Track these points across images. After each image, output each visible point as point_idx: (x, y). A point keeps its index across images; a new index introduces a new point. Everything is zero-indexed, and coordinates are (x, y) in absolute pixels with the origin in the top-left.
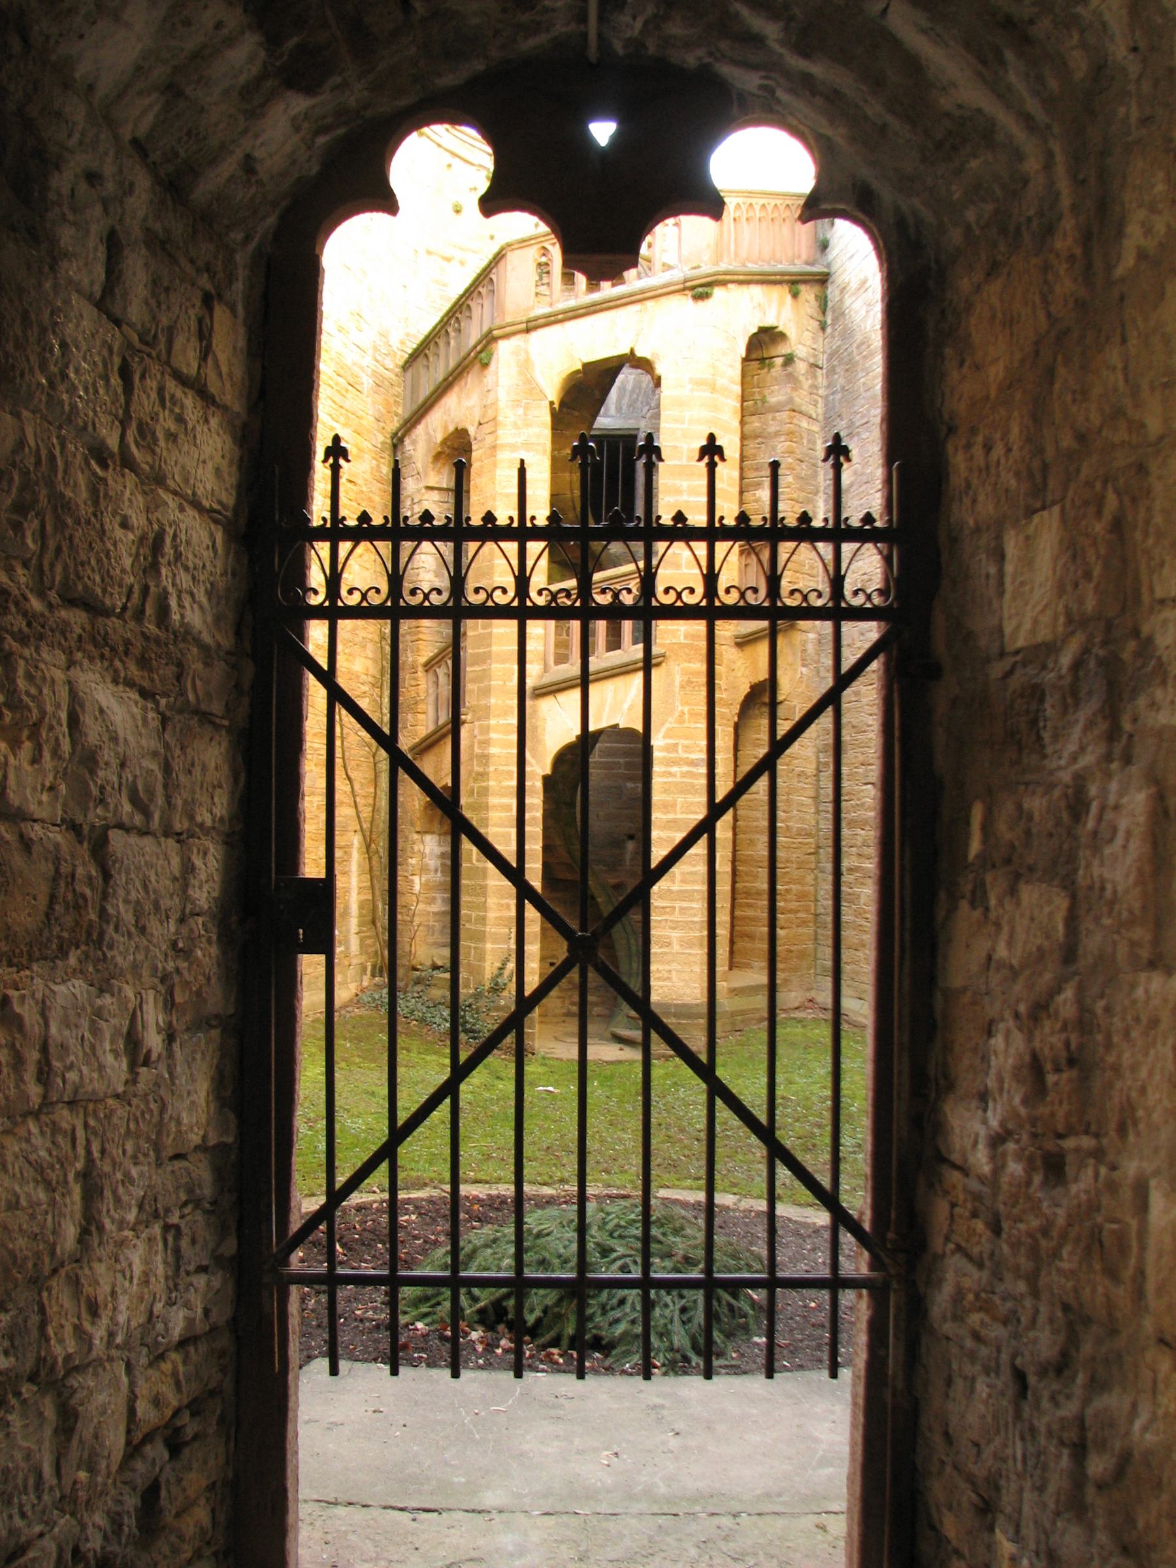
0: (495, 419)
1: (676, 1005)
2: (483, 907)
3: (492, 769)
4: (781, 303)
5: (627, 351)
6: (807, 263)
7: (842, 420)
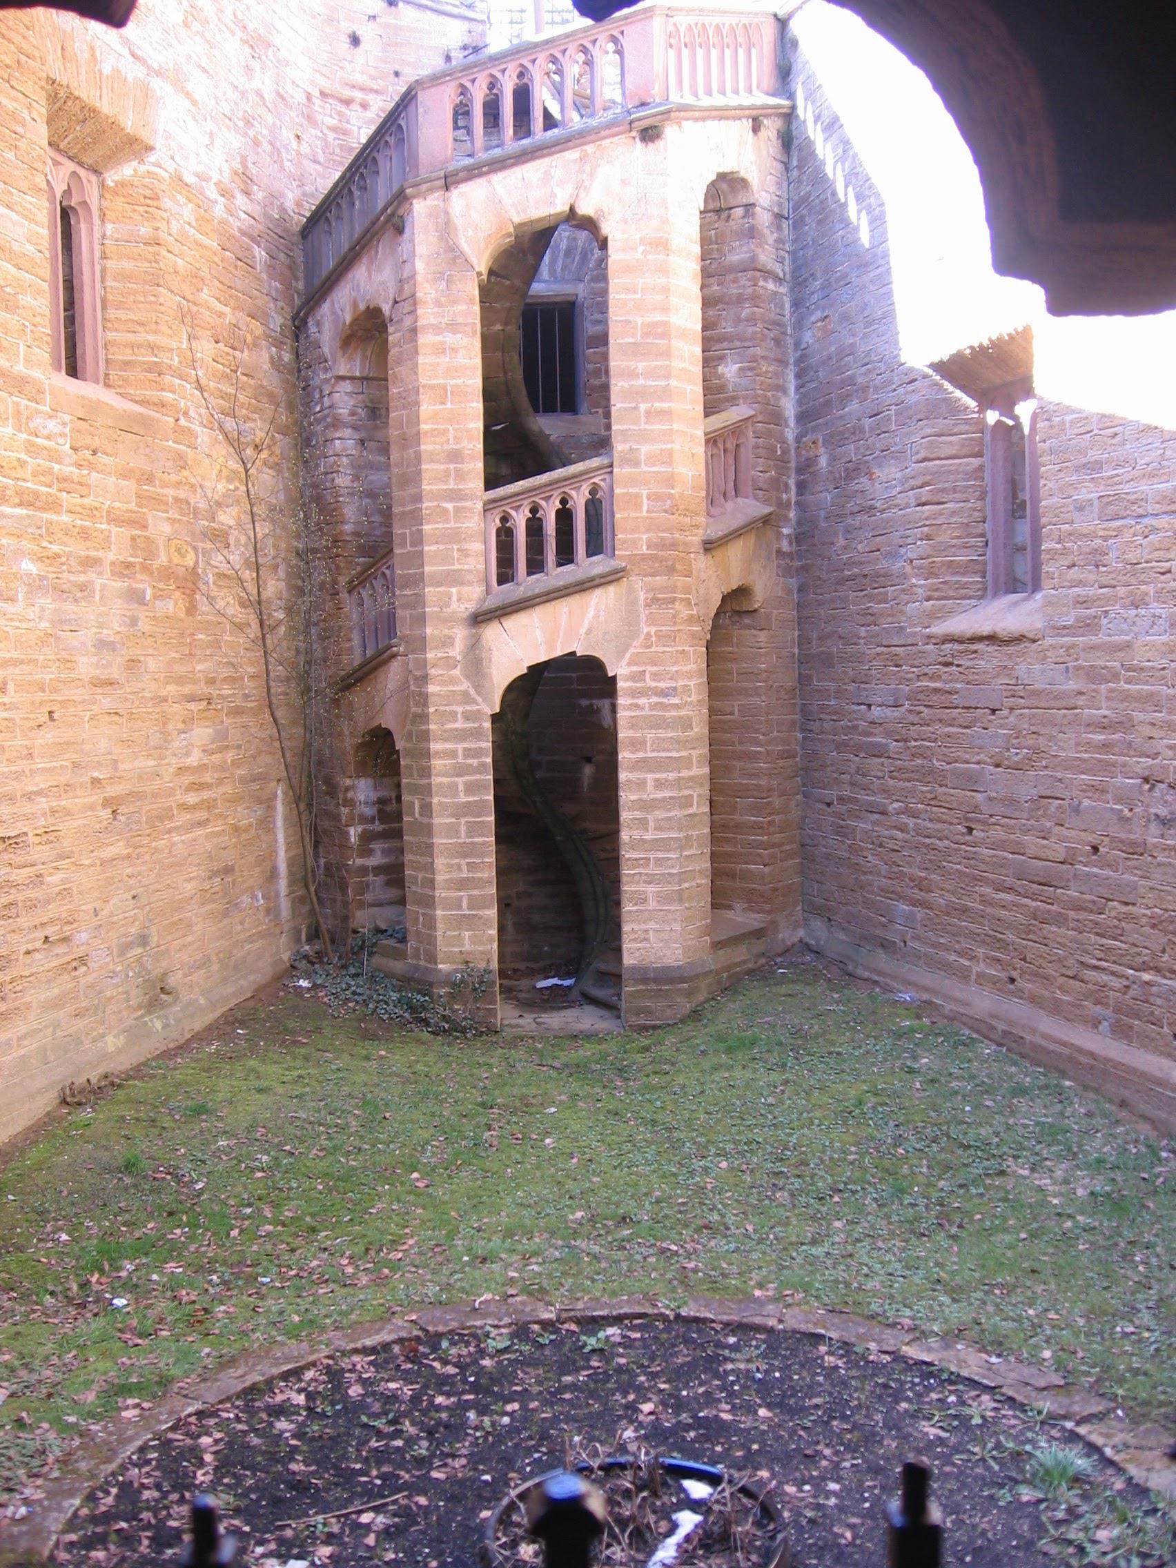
0: (413, 296)
1: (655, 969)
2: (431, 868)
3: (432, 710)
5: (567, 208)
7: (815, 279)
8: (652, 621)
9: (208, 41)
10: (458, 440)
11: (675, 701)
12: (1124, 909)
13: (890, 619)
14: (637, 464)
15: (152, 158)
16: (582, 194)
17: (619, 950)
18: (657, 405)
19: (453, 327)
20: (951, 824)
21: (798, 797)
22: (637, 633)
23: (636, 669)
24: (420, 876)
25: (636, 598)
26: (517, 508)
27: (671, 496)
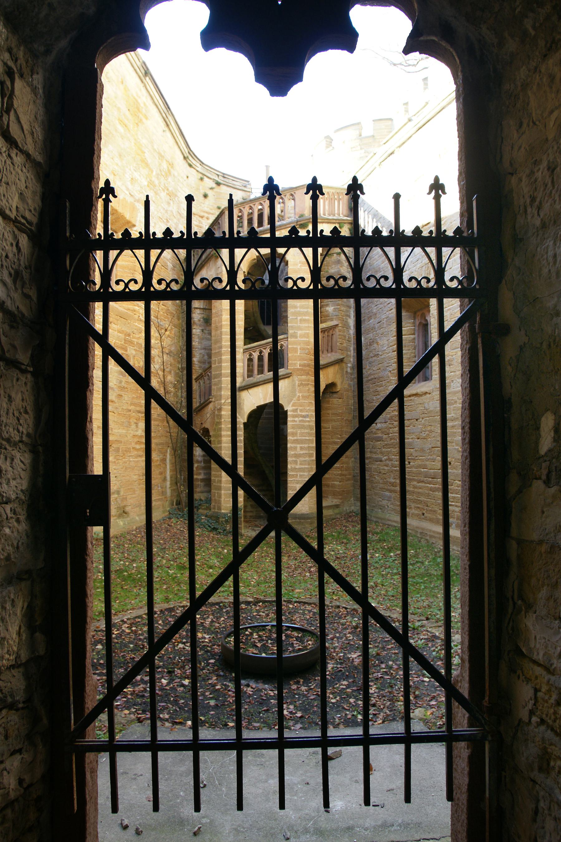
3: (223, 420)
8: (300, 392)
9: (155, 192)
11: (308, 419)
14: (296, 337)
18: (304, 317)
21: (353, 459)
22: (294, 396)
23: (294, 408)
24: (217, 479)
25: (295, 383)
26: (254, 352)
27: (308, 349)
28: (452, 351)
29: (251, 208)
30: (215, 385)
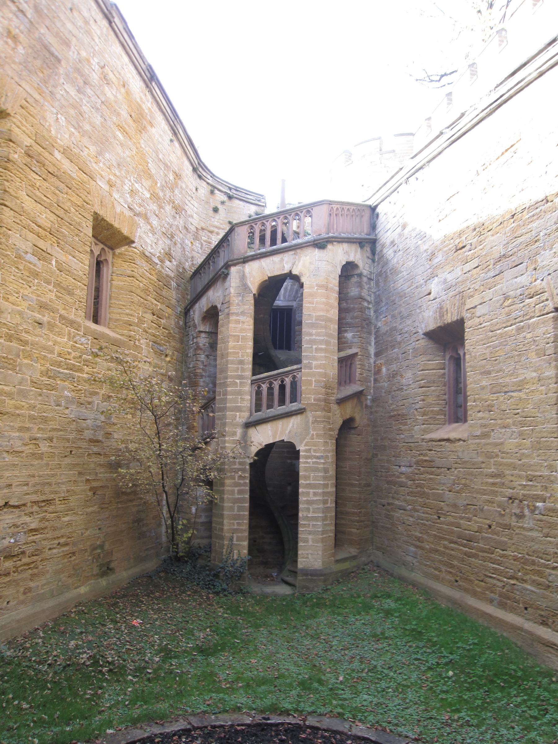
1: (311, 570)
2: (222, 524)
4: (356, 252)
6: (367, 235)
8: (314, 429)
9: (159, 205)
10: (243, 356)
12: (501, 552)
13: (408, 432)
15: (134, 245)
16: (295, 267)
17: (296, 561)
19: (243, 313)
20: (431, 515)
23: (307, 448)
24: (218, 527)
26: (264, 383)
28: (492, 395)
29: (263, 224)
30: (219, 419)
